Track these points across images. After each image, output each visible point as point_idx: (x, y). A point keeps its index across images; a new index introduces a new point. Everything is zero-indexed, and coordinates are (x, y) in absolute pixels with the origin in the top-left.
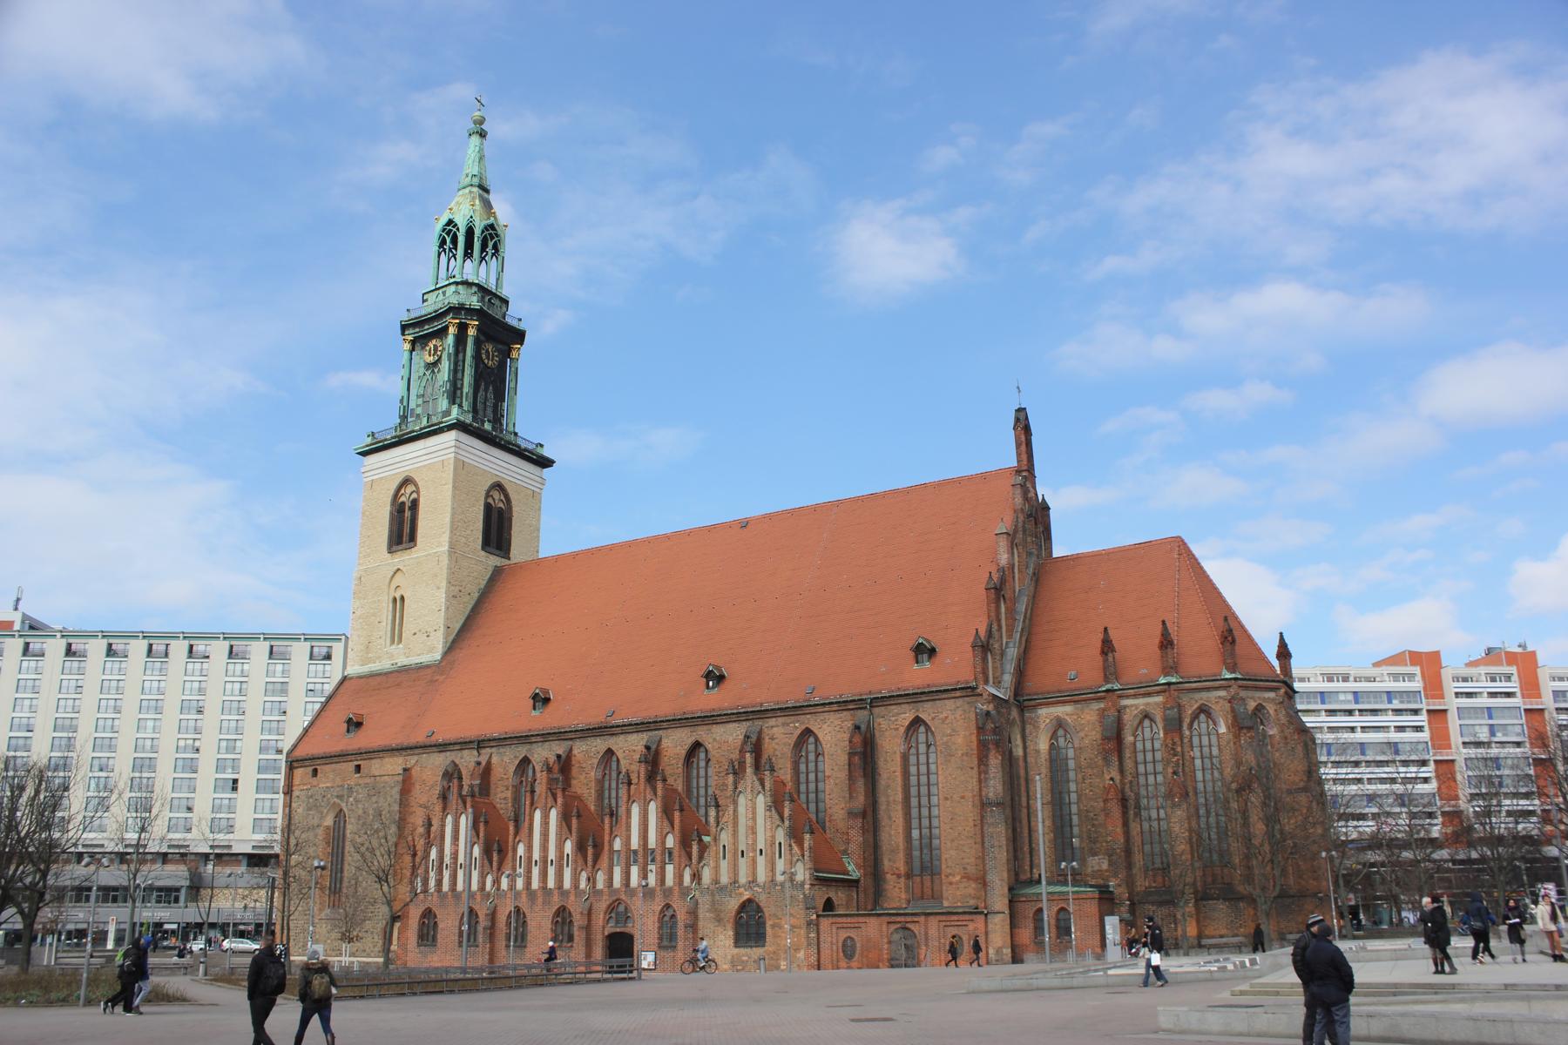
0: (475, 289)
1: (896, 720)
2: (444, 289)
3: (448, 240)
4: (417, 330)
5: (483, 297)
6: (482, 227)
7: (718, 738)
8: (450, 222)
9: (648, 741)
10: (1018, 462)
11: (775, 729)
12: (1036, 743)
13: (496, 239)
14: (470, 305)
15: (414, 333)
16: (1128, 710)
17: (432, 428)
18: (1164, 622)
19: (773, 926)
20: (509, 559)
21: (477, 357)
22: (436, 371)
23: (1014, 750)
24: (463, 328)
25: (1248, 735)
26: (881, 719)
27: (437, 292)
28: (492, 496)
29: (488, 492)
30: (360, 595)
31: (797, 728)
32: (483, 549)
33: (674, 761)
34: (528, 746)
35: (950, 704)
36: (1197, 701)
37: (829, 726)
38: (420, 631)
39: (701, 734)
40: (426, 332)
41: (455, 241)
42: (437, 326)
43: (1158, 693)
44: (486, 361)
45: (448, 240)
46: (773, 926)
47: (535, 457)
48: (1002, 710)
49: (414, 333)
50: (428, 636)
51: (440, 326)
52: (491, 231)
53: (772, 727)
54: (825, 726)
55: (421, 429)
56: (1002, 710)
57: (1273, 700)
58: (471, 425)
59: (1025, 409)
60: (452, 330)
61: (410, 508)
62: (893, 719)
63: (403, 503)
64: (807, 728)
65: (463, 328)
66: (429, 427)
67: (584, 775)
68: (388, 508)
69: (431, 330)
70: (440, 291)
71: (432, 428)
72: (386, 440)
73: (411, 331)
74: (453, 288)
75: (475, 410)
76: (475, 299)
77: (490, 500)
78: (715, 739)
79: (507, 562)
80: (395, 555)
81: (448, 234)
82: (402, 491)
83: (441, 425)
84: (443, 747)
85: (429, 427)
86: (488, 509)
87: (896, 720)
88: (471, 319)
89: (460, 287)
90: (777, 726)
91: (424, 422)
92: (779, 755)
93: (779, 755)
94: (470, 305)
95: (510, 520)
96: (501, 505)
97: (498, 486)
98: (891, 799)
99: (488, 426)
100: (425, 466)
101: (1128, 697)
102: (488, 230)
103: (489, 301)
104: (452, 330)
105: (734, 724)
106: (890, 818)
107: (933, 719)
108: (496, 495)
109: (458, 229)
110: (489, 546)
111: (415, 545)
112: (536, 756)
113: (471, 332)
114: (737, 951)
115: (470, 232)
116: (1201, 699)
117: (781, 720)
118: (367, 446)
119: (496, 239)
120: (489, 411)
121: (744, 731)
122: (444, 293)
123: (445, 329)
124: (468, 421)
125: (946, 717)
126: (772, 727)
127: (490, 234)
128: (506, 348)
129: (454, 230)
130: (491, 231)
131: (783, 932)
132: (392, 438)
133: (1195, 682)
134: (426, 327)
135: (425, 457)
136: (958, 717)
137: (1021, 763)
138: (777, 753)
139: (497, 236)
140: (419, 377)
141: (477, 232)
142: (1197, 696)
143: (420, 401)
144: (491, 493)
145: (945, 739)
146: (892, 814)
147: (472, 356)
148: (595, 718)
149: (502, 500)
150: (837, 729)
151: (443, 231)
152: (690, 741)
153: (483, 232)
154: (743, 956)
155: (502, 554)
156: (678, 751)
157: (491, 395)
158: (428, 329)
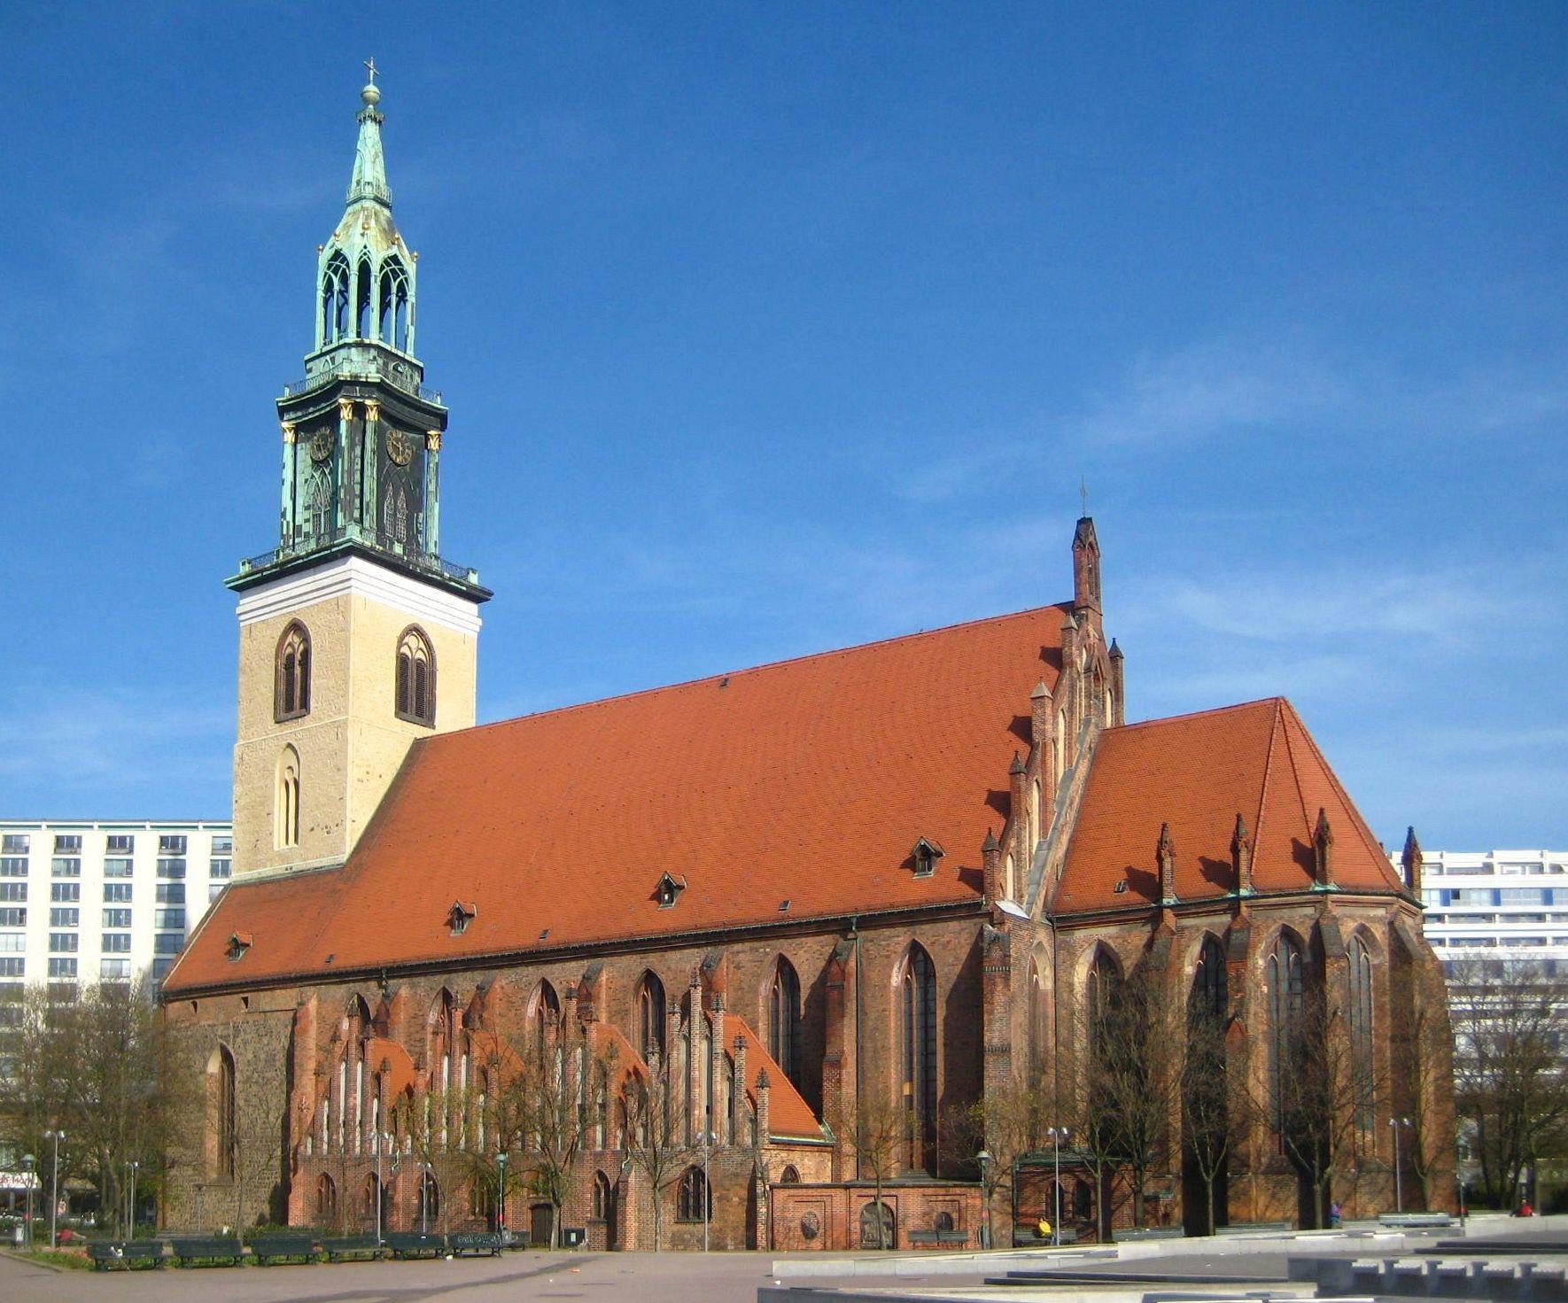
0: (373, 353)
1: (888, 945)
2: (333, 354)
3: (336, 280)
4: (300, 414)
5: (385, 364)
6: (380, 261)
7: (673, 967)
8: (338, 255)
9: (588, 970)
10: (1076, 594)
11: (741, 955)
12: (1070, 973)
13: (402, 277)
14: (367, 377)
15: (295, 419)
16: (1186, 932)
17: (322, 554)
18: (1239, 817)
19: (720, 1199)
20: (434, 728)
21: (381, 452)
23: (1041, 983)
24: (359, 410)
25: (1336, 965)
26: (870, 944)
27: (323, 359)
28: (407, 644)
29: (401, 639)
31: (768, 954)
32: (397, 715)
33: (621, 995)
34: (445, 976)
35: (953, 926)
36: (1275, 921)
37: (805, 951)
39: (653, 961)
40: (310, 417)
41: (345, 280)
42: (325, 408)
43: (1225, 911)
44: (394, 456)
45: (336, 280)
46: (720, 1199)
47: (464, 588)
48: (1021, 933)
49: (295, 419)
51: (328, 409)
52: (393, 266)
53: (738, 952)
54: (801, 952)
55: (308, 555)
56: (1021, 933)
57: (1379, 920)
58: (372, 548)
59: (1090, 519)
60: (346, 414)
62: (883, 943)
64: (781, 954)
65: (359, 410)
66: (318, 551)
67: (514, 1012)
69: (317, 414)
70: (328, 357)
71: (322, 554)
72: (266, 569)
73: (292, 415)
74: (343, 353)
75: (381, 528)
76: (373, 368)
77: (405, 650)
78: (669, 968)
79: (427, 732)
80: (283, 726)
81: (335, 273)
83: (334, 550)
84: (342, 977)
85: (318, 551)
86: (403, 661)
87: (888, 945)
88: (370, 398)
89: (353, 350)
90: (743, 952)
91: (312, 545)
92: (746, 988)
93: (746, 988)
94: (367, 377)
95: (433, 674)
96: (420, 655)
97: (415, 630)
98: (879, 1045)
99: (398, 549)
101: (1187, 915)
102: (389, 265)
103: (395, 368)
104: (346, 414)
105: (692, 950)
106: (877, 1067)
107: (933, 943)
108: (412, 640)
110: (405, 710)
111: (309, 713)
112: (455, 987)
113: (372, 416)
114: (676, 1228)
115: (364, 269)
116: (1281, 918)
117: (748, 945)
118: (241, 578)
119: (402, 277)
120: (402, 528)
121: (703, 957)
122: (333, 359)
123: (338, 409)
124: (368, 543)
125: (949, 942)
126: (738, 952)
127: (393, 271)
128: (423, 436)
129: (343, 266)
130: (393, 266)
131: (730, 1206)
132: (272, 567)
133: (1274, 896)
134: (311, 410)
135: (315, 594)
136: (963, 941)
137: (1051, 1001)
138: (743, 985)
139: (403, 272)
140: (306, 481)
141: (375, 268)
142: (1277, 914)
144: (406, 640)
145: (946, 970)
146: (880, 1063)
147: (373, 451)
148: (525, 939)
149: (421, 649)
150: (816, 956)
151: (329, 268)
152: (642, 969)
153: (382, 268)
154: (685, 1233)
155: (424, 720)
156: (626, 983)
157: (401, 503)
158: (313, 413)
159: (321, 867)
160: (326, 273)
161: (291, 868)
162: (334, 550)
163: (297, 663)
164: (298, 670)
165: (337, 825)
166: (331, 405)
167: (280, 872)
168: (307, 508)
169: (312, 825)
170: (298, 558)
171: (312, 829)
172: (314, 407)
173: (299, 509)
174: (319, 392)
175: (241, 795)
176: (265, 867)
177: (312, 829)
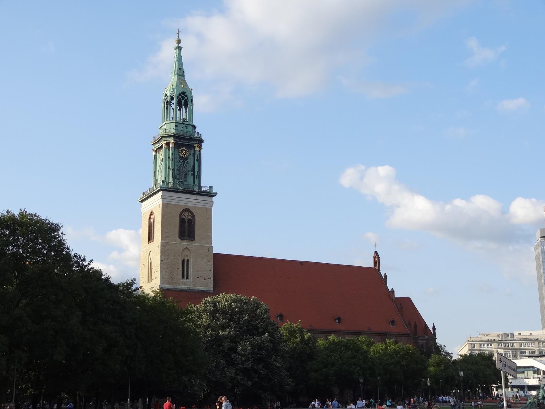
2: (186, 125)
4: (178, 140)
22: (186, 162)
30: (165, 254)
38: (201, 277)
40: (182, 143)
49: (177, 141)
50: (204, 280)
61: (188, 222)
63: (183, 219)
68: (178, 219)
69: (184, 143)
70: (184, 125)
82: (184, 214)
83: (209, 194)
100: (197, 207)
109: (188, 98)
111: (194, 240)
122: (187, 128)
135: (197, 204)
140: (177, 161)
143: (178, 172)
159: (203, 290)
160: (178, 97)
161: (189, 288)
162: (209, 194)
163: (187, 222)
164: (187, 224)
165: (209, 278)
166: (191, 143)
167: (184, 288)
168: (178, 170)
169: (198, 276)
170: (195, 191)
171: (198, 277)
172: (183, 140)
173: (175, 170)
174: (189, 138)
175: (164, 259)
176: (177, 285)
177: (198, 277)
